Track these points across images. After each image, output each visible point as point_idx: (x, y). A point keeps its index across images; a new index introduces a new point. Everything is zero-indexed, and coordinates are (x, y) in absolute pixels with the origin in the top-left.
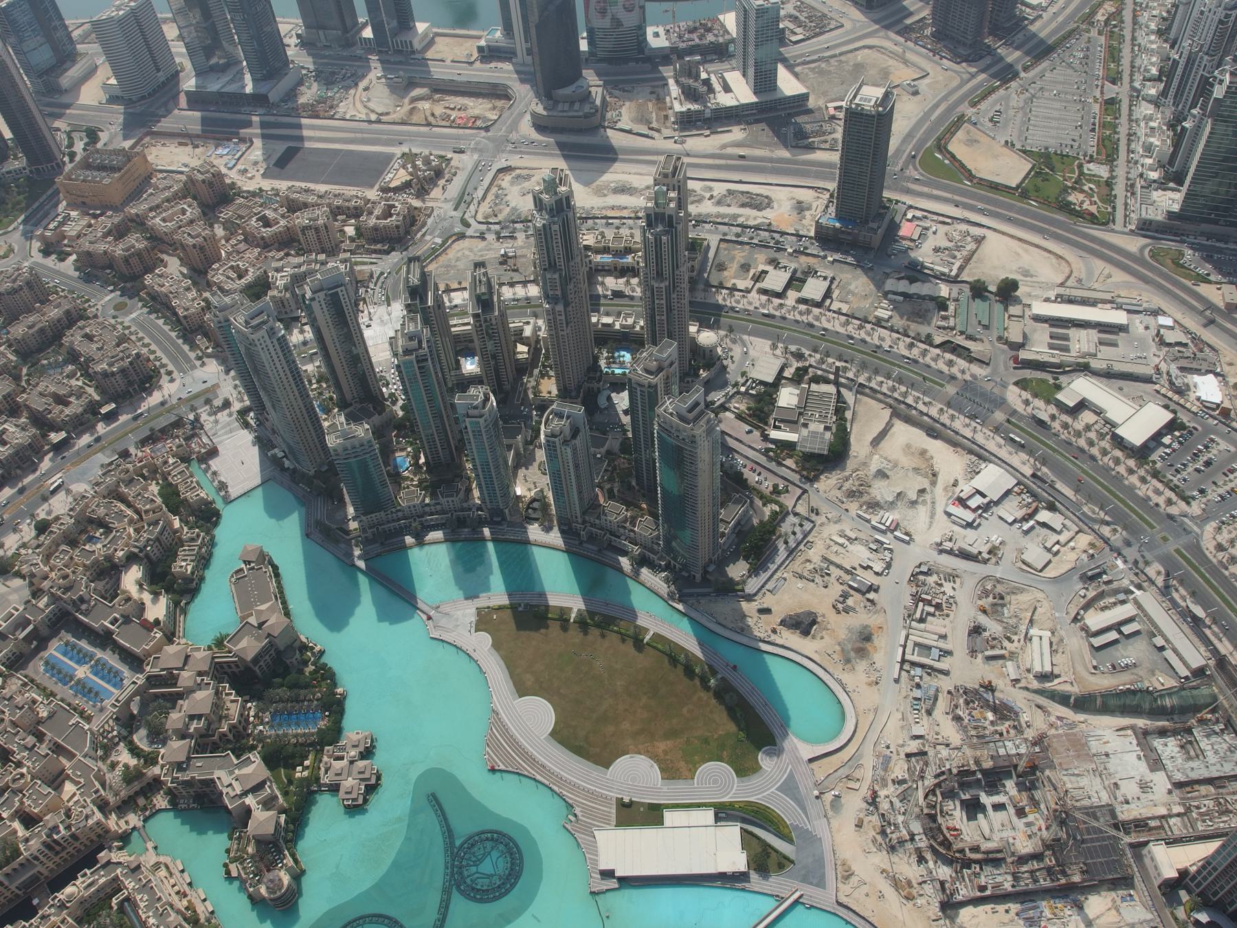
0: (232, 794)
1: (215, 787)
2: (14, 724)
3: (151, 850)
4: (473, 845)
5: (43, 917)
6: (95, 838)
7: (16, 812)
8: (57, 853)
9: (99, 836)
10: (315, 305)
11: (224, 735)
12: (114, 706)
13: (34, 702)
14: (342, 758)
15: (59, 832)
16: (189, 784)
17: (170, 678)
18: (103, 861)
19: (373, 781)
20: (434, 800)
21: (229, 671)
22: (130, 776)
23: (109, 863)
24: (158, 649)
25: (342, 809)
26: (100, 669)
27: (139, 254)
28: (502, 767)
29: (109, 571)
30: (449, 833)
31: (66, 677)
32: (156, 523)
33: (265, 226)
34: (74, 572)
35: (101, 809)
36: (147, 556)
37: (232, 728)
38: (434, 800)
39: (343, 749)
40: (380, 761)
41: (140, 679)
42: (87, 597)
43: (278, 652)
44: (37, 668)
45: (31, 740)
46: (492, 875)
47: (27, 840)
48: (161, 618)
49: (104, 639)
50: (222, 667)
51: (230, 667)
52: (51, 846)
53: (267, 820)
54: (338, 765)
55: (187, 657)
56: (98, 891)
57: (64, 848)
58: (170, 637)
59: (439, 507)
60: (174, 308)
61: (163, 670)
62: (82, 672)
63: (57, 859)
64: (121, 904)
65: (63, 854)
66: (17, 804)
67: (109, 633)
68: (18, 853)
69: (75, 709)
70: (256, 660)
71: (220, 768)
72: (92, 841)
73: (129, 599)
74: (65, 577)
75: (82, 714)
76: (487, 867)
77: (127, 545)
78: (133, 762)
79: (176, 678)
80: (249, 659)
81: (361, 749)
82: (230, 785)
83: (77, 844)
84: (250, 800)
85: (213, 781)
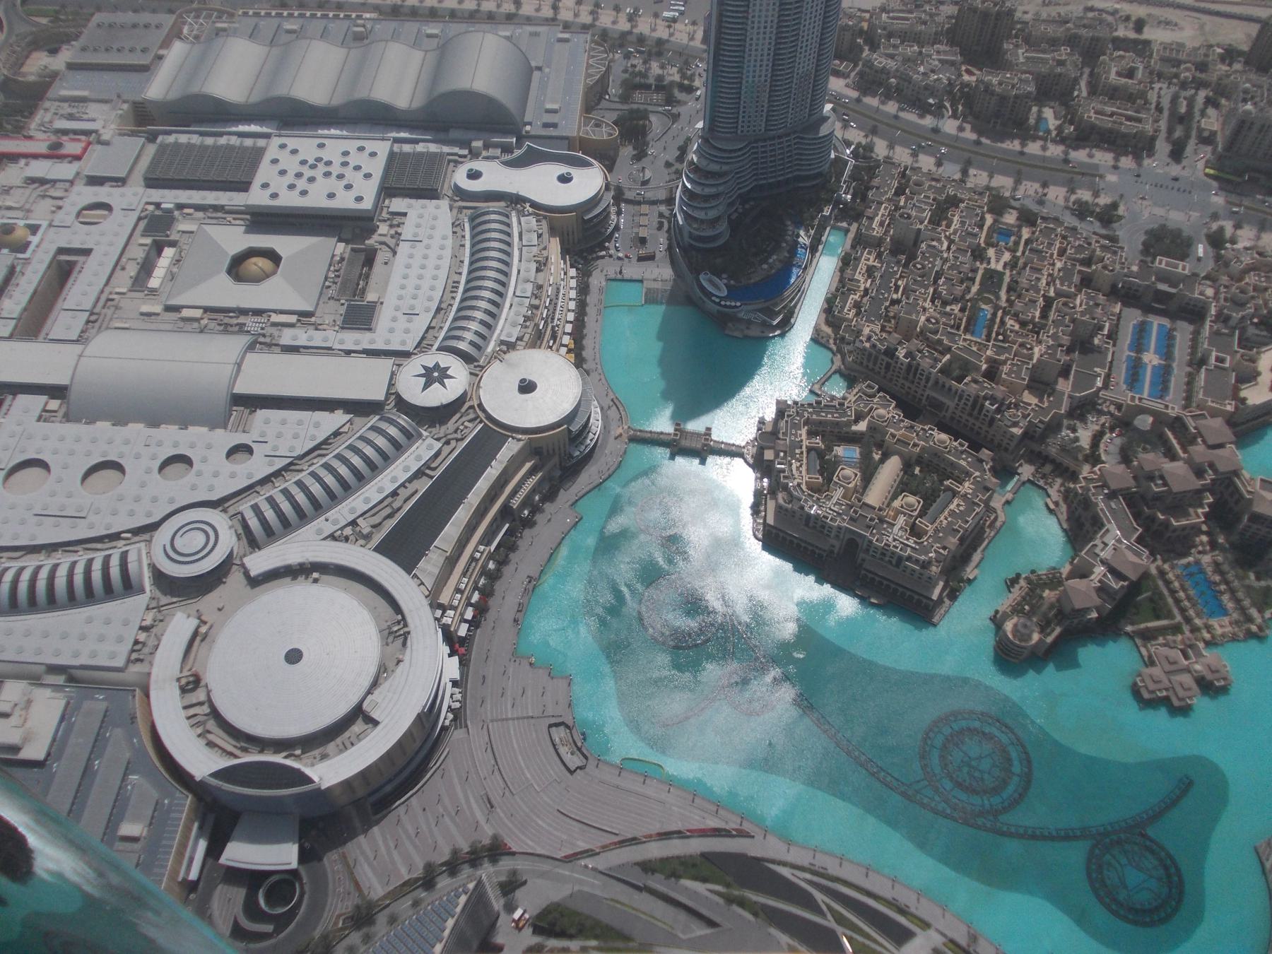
0: (1097, 551)
1: (1096, 532)
2: (1073, 321)
3: (1004, 500)
4: (1152, 852)
5: (912, 427)
7: (995, 361)
8: (970, 415)
11: (1153, 519)
12: (1133, 398)
13: (1101, 328)
14: (1186, 657)
16: (1087, 504)
17: (1188, 440)
19: (1176, 703)
20: (1186, 786)
22: (1070, 449)
23: (981, 461)
24: (1214, 413)
25: (1130, 681)
26: (1164, 374)
30: (1156, 815)
31: (1139, 345)
34: (1253, 298)
35: (1025, 434)
37: (1166, 524)
38: (1186, 786)
39: (1199, 654)
40: (1201, 704)
41: (1174, 410)
42: (1232, 323)
44: (1133, 317)
45: (1066, 340)
46: (1125, 887)
47: (975, 381)
48: (1250, 402)
49: (1198, 362)
52: (977, 403)
54: (1176, 654)
55: (1221, 446)
56: (952, 464)
58: (1231, 421)
61: (1195, 428)
62: (1151, 359)
63: (965, 417)
64: (948, 489)
65: (972, 420)
66: (1003, 358)
67: (1203, 361)
68: (960, 379)
69: (1110, 369)
73: (1253, 360)
74: (1242, 292)
75: (1108, 376)
76: (1133, 877)
79: (1193, 441)
81: (1209, 677)
82: (1106, 545)
83: (985, 428)
84: (1100, 570)
85: (1103, 525)
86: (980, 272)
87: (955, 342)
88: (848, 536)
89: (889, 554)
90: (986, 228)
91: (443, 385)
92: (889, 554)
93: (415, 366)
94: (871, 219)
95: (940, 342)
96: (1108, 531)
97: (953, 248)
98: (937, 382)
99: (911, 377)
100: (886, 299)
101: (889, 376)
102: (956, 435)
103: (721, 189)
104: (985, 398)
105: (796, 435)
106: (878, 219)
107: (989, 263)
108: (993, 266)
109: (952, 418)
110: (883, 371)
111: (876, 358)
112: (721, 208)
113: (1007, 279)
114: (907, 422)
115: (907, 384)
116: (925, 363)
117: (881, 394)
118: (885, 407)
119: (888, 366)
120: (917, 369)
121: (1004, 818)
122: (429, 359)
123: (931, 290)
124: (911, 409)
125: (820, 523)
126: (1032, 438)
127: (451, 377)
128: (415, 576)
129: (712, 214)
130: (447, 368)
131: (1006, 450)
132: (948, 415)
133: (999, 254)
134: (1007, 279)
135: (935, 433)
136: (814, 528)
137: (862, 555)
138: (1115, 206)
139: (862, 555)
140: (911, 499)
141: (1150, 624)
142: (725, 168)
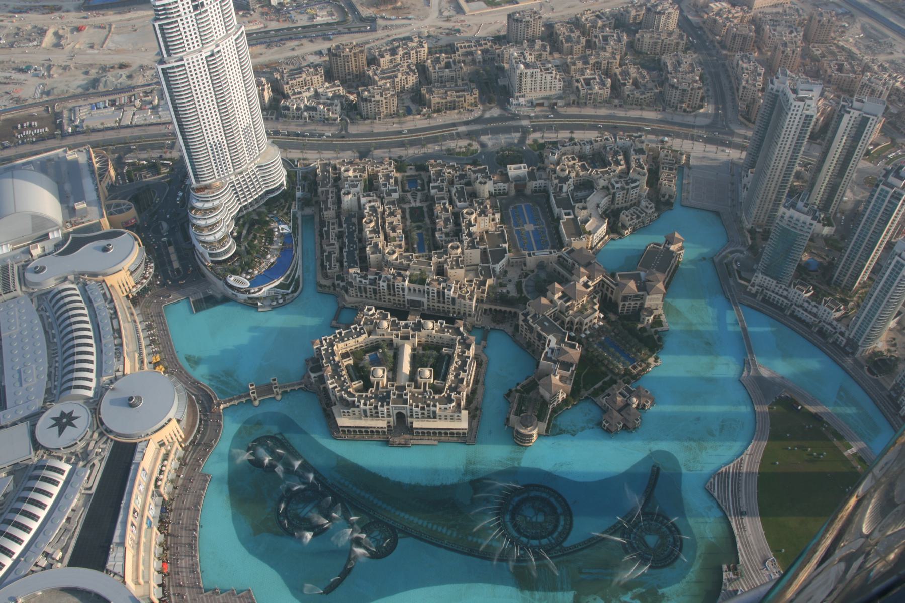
1: (544, 344)
6: (462, 312)
8: (439, 302)
9: (464, 313)
10: (846, 117)
15: (450, 290)
18: (456, 325)
21: (605, 292)
27: (745, 38)
28: (716, 495)
29: (586, 186)
32: (634, 181)
33: (837, 70)
36: (614, 194)
43: (641, 306)
50: (603, 286)
51: (607, 289)
52: (441, 294)
53: (556, 385)
57: (444, 302)
59: (815, 310)
60: (741, 79)
63: (436, 304)
65: (441, 305)
66: (443, 259)
70: (625, 299)
71: (554, 336)
72: (459, 313)
77: (609, 180)
78: (514, 293)
80: (626, 292)
83: (451, 306)
86: (408, 211)
87: (411, 261)
88: (395, 411)
89: (426, 412)
90: (399, 184)
91: (73, 425)
92: (426, 412)
93: (45, 421)
94: (326, 202)
95: (401, 263)
96: (549, 341)
97: (385, 201)
98: (410, 290)
99: (392, 292)
100: (356, 249)
101: (377, 297)
102: (435, 318)
103: (218, 217)
104: (444, 288)
105: (334, 360)
106: (330, 200)
107: (410, 202)
108: (413, 204)
109: (429, 308)
110: (373, 296)
111: (365, 288)
112: (223, 230)
113: (425, 209)
114: (403, 323)
115: (392, 298)
116: (398, 282)
117: (378, 311)
118: (385, 317)
119: (375, 290)
120: (394, 286)
121: (566, 544)
122: (55, 410)
123: (381, 235)
124: (400, 313)
125: (374, 411)
126: (482, 301)
127: (77, 417)
128: (107, 571)
129: (219, 235)
130: (71, 413)
131: (470, 315)
132: (426, 307)
133: (414, 197)
134: (425, 209)
135: (422, 321)
136: (371, 415)
137: (409, 419)
138: (470, 145)
139: (409, 419)
140: (427, 372)
141: (597, 386)
142: (216, 203)
